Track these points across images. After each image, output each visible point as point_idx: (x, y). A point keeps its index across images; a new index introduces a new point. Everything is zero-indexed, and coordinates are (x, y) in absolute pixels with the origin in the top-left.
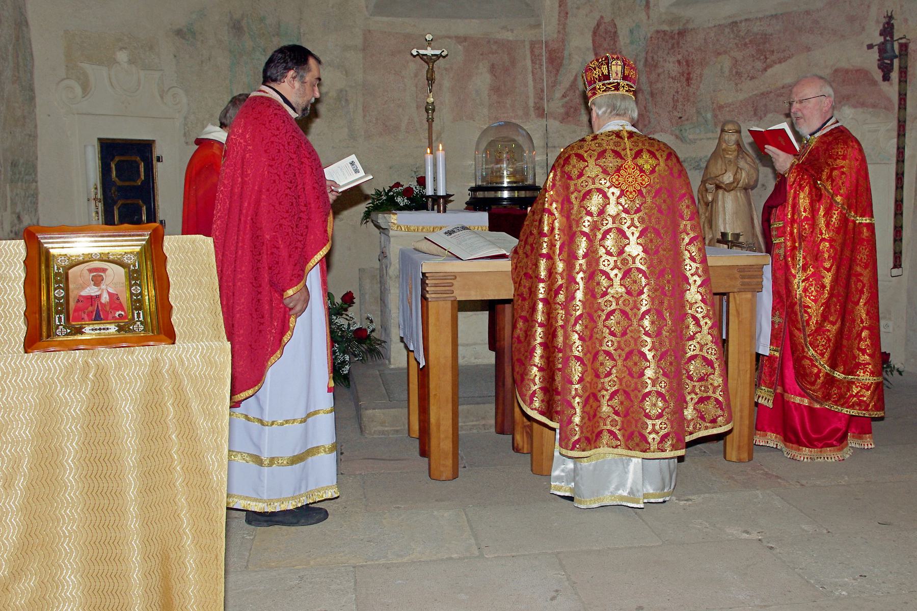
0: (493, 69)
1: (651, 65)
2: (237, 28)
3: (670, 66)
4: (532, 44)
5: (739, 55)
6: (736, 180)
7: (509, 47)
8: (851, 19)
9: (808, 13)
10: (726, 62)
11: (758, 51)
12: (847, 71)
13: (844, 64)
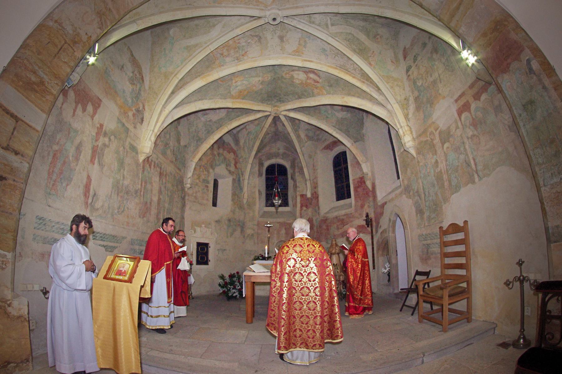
0: (285, 229)
1: (320, 227)
2: (229, 220)
3: (324, 227)
5: (338, 224)
6: (335, 252)
8: (360, 214)
10: (335, 226)
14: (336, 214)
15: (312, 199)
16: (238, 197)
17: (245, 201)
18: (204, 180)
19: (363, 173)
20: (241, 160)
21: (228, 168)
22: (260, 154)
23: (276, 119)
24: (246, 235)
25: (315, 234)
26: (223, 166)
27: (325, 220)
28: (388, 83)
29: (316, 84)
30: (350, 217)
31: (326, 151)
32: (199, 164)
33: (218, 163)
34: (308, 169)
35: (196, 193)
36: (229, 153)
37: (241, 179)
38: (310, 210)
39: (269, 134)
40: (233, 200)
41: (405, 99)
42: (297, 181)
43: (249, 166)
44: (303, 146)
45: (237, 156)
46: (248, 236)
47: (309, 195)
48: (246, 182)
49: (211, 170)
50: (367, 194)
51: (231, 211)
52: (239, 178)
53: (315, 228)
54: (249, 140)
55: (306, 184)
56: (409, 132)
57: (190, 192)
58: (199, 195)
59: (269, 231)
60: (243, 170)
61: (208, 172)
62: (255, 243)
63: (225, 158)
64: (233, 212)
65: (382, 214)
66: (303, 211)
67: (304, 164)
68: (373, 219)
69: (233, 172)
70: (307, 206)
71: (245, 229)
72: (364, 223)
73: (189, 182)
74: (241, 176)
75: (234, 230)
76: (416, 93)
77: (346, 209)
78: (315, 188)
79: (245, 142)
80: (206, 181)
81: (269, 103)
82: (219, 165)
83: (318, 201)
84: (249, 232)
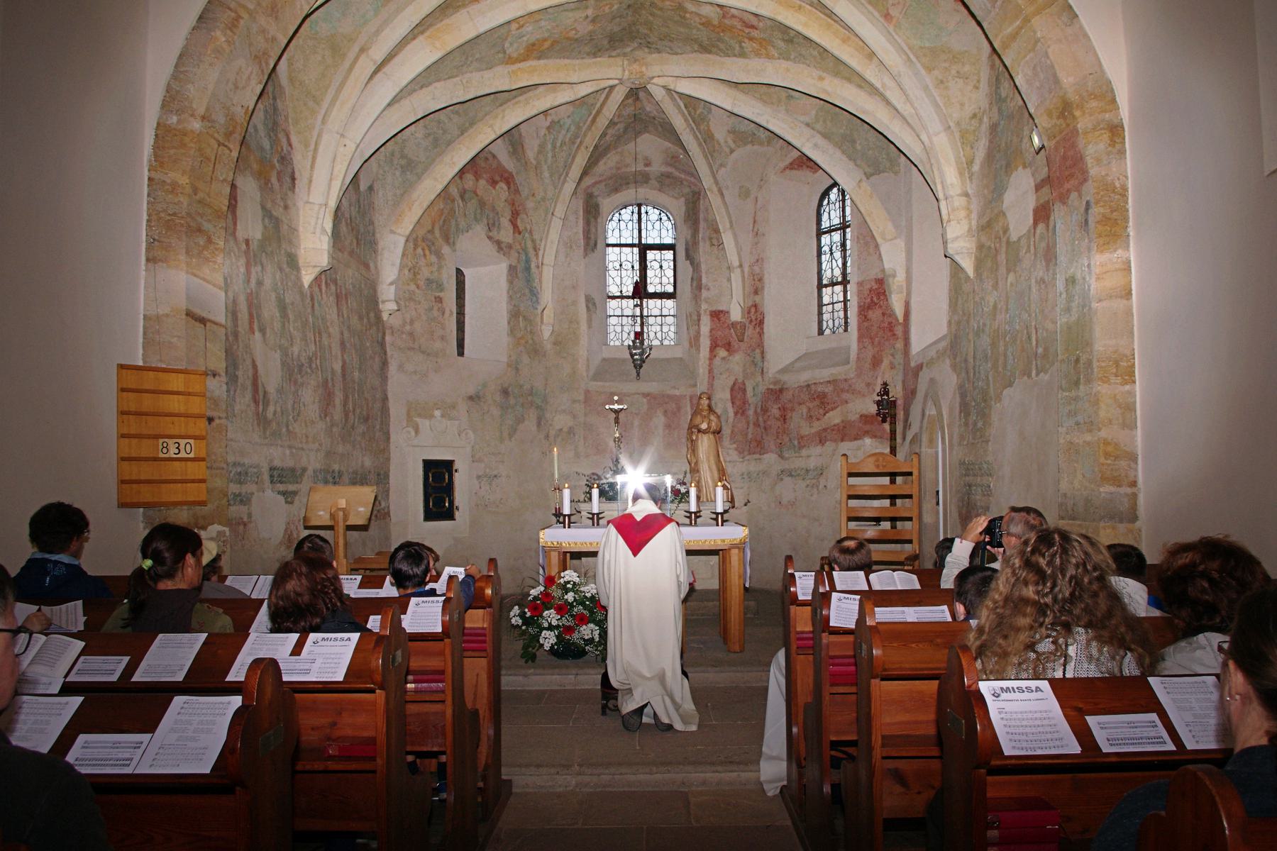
1: (765, 410)
2: (505, 392)
3: (775, 411)
4: (691, 398)
5: (811, 405)
7: (677, 399)
8: (868, 385)
9: (846, 380)
10: (805, 410)
11: (822, 403)
12: (866, 416)
13: (864, 412)
14: (805, 377)
15: (744, 327)
16: (525, 318)
17: (546, 332)
18: (429, 281)
19: (883, 270)
20: (530, 204)
21: (494, 233)
22: (588, 181)
23: (636, 93)
24: (552, 433)
25: (750, 430)
26: (480, 230)
27: (777, 392)
28: (929, 70)
29: (747, 30)
30: (842, 390)
31: (794, 172)
32: (414, 241)
33: (463, 224)
34: (735, 236)
35: (412, 322)
36: (494, 183)
37: (533, 265)
38: (738, 358)
39: (615, 124)
40: (512, 331)
41: (974, 116)
42: (703, 267)
43: (556, 224)
44: (721, 165)
45: (517, 191)
46: (556, 436)
47: (736, 315)
48: (548, 274)
49: (446, 250)
50: (891, 327)
51: (509, 365)
52: (528, 261)
53: (751, 412)
54: (554, 147)
55: (729, 280)
56: (963, 214)
57: (395, 321)
58: (418, 327)
59: (617, 421)
60: (536, 237)
61: (439, 255)
62: (577, 455)
63: (482, 204)
64: (515, 366)
65: (914, 392)
66: (717, 361)
67: (723, 224)
68: (900, 402)
69: (510, 247)
70: (728, 347)
71: (548, 415)
72: (873, 409)
73: (392, 297)
74: (531, 252)
75: (520, 420)
76: (996, 117)
77: (833, 366)
78: (756, 292)
79: (542, 147)
80: (434, 284)
81: (614, 54)
82: (468, 228)
83: (761, 334)
84: (561, 421)
